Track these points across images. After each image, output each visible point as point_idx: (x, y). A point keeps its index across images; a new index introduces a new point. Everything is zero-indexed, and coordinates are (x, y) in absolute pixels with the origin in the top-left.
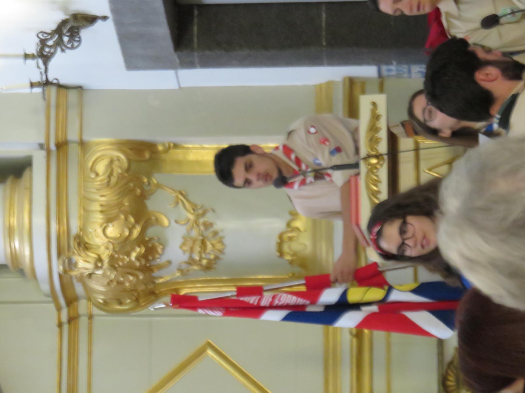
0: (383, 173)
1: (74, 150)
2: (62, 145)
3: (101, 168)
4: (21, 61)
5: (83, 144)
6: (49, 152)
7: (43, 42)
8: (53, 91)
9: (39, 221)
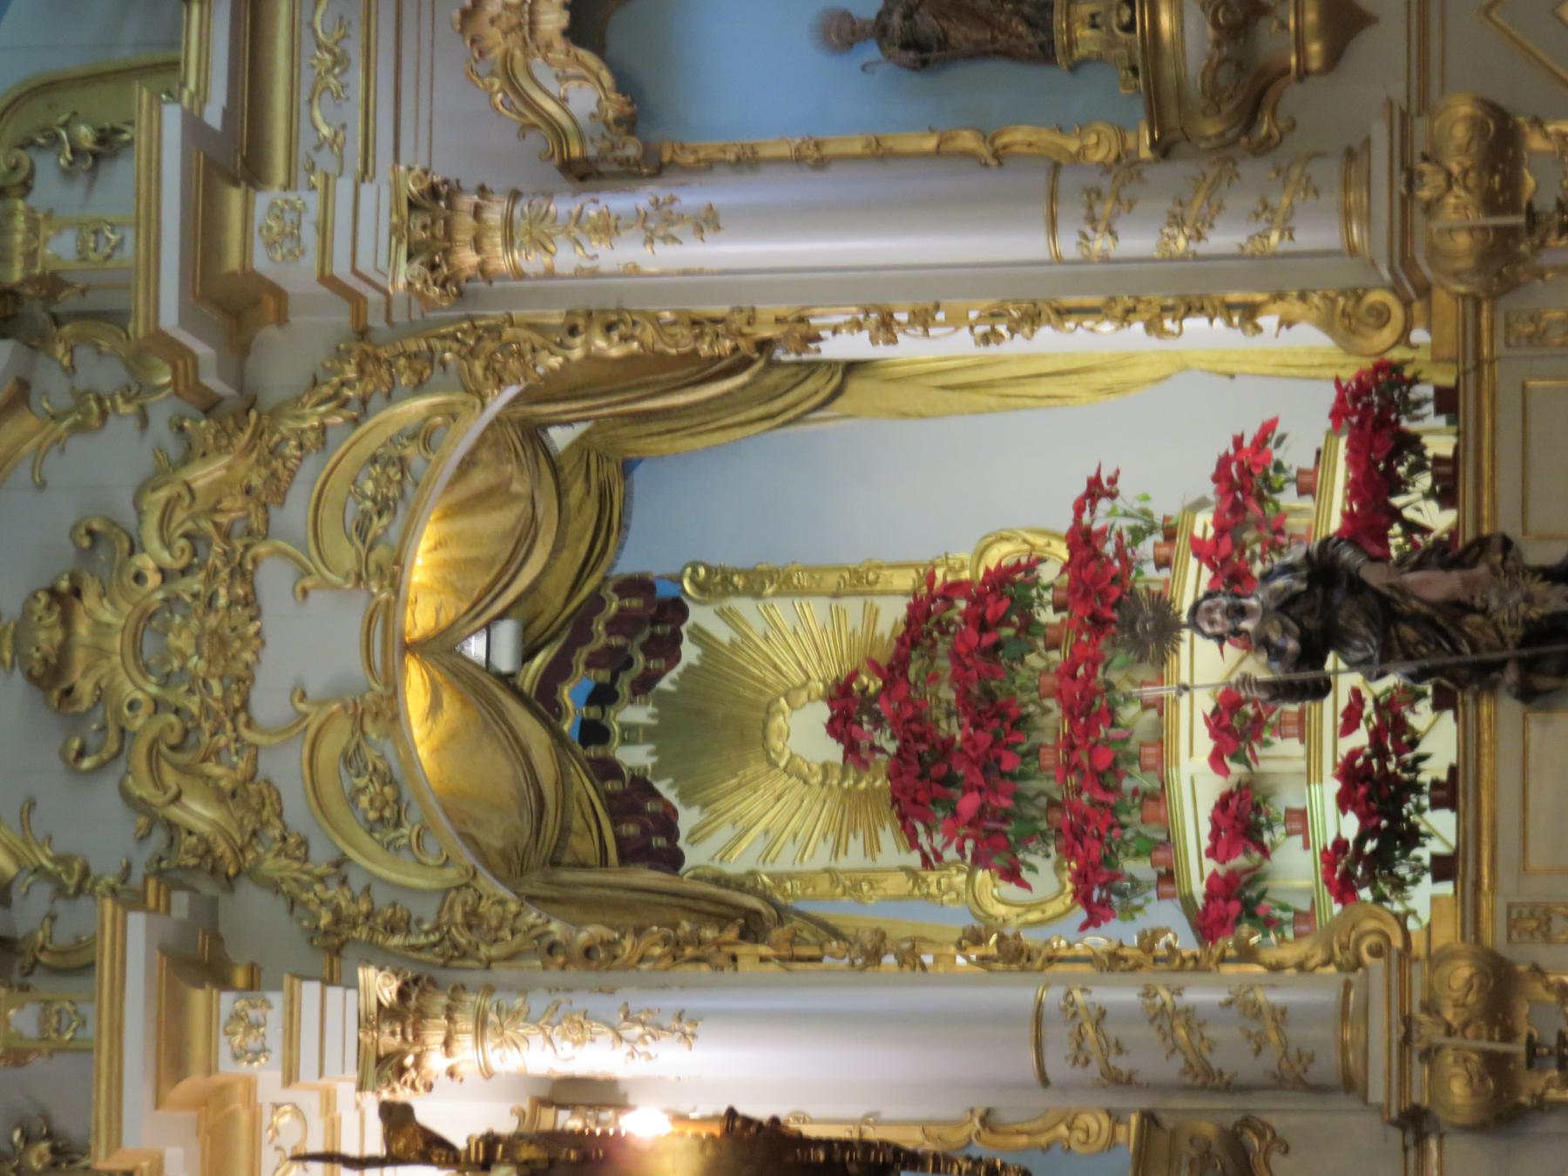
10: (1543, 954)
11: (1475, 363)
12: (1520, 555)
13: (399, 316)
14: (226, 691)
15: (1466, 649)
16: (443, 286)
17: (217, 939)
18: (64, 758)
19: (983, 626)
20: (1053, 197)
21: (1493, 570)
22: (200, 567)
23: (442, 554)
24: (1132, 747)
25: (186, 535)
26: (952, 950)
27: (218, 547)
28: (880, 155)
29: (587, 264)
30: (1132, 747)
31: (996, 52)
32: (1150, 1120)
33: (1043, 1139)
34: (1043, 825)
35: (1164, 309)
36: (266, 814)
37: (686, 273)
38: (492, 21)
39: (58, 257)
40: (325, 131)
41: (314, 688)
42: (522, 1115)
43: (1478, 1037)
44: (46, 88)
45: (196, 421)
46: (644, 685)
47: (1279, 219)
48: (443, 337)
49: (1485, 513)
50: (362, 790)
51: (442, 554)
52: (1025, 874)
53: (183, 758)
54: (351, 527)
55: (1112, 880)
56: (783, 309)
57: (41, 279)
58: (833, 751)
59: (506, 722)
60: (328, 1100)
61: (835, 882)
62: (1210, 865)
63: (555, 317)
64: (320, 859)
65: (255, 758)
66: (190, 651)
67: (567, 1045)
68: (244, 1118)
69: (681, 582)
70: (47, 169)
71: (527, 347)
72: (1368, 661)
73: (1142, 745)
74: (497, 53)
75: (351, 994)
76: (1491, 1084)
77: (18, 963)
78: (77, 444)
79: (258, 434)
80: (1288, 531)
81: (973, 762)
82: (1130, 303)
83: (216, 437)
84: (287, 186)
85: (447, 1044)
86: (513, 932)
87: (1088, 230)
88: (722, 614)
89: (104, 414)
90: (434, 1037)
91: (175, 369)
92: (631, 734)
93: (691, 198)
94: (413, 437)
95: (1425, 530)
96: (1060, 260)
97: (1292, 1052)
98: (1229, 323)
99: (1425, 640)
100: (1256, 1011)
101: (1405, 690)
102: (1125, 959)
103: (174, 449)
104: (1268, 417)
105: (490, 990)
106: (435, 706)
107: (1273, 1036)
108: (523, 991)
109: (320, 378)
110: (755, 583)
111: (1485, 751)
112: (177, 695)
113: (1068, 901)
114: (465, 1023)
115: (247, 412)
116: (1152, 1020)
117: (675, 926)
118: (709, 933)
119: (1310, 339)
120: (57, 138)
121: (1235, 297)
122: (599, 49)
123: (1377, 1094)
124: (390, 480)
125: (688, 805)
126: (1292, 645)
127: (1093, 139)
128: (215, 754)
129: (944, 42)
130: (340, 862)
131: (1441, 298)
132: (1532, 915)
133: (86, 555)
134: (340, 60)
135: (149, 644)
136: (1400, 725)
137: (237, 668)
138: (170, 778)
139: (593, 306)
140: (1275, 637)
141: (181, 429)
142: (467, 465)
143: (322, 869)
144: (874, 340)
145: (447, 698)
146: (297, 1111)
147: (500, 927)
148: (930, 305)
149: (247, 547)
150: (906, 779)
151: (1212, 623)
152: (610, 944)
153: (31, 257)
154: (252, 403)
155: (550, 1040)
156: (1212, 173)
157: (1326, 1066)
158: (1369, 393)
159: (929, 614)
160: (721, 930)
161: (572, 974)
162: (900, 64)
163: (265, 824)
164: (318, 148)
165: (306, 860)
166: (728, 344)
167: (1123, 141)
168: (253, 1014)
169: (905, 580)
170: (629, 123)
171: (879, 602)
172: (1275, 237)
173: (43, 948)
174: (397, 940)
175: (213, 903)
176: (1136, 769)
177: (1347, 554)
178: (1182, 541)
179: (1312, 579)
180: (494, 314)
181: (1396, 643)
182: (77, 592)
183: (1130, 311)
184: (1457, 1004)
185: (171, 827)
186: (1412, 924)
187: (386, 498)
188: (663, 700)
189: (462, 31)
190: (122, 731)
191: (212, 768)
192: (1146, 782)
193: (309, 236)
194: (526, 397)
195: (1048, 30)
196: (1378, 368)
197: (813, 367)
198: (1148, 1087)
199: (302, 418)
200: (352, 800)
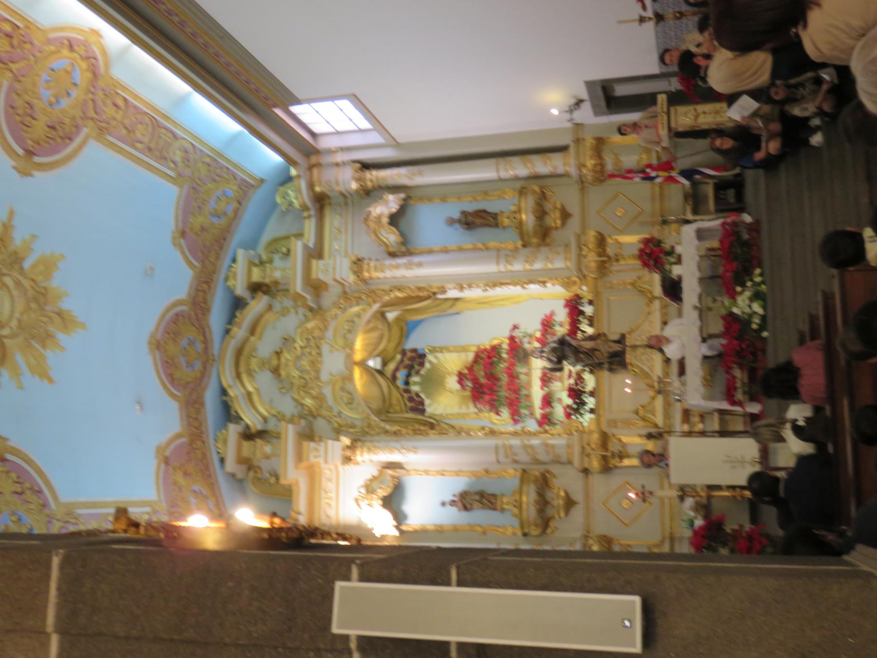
0: (665, 118)
5: (584, 139)
10: (615, 431)
11: (597, 293)
17: (312, 430)
28: (461, 249)
32: (524, 471)
44: (276, 240)
46: (417, 373)
52: (500, 413)
53: (305, 389)
55: (519, 414)
56: (438, 284)
58: (457, 386)
62: (542, 412)
64: (335, 411)
70: (276, 257)
90: (358, 453)
92: (415, 383)
93: (416, 259)
94: (355, 315)
96: (501, 272)
100: (546, 445)
105: (371, 441)
106: (361, 377)
108: (379, 441)
110: (442, 349)
118: (422, 428)
120: (277, 251)
121: (541, 279)
126: (555, 359)
128: (312, 388)
130: (340, 413)
131: (589, 279)
133: (284, 344)
134: (340, 231)
142: (369, 322)
146: (330, 470)
152: (399, 431)
154: (320, 308)
157: (564, 458)
169: (474, 349)
174: (352, 430)
180: (373, 287)
182: (281, 352)
184: (595, 443)
185: (302, 405)
188: (422, 376)
193: (331, 270)
194: (383, 306)
197: (447, 300)
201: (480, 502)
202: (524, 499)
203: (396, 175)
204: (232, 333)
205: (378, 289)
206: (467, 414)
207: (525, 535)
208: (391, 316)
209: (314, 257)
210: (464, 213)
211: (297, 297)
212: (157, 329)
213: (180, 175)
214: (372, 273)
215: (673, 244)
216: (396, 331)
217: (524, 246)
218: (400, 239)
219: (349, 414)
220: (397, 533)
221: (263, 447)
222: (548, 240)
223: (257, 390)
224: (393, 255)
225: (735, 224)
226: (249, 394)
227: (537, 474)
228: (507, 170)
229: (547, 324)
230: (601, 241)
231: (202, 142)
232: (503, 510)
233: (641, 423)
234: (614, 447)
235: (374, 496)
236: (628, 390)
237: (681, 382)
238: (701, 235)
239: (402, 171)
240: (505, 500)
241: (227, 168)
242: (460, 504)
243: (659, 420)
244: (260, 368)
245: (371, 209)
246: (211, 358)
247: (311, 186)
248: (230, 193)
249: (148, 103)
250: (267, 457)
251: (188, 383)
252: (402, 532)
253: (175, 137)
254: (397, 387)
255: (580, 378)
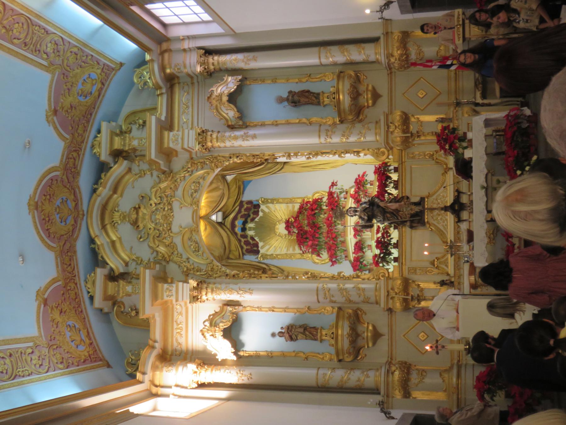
0: (461, 29)
1: (390, 34)
2: (387, 33)
3: (396, 38)
4: (376, 13)
5: (392, 33)
6: (384, 35)
7: (381, 8)
8: (385, 20)
9: (382, 51)
10: (414, 277)
11: (402, 163)
12: (410, 200)
13: (198, 155)
14: (167, 226)
15: (400, 218)
16: (206, 149)
17: (165, 272)
18: (137, 238)
19: (312, 210)
20: (320, 131)
21: (405, 204)
22: (162, 203)
23: (207, 200)
24: (339, 233)
25: (159, 197)
26: (302, 275)
27: (165, 199)
28: (288, 123)
29: (232, 145)
30: (339, 233)
31: (309, 103)
32: (340, 309)
33: (319, 312)
34: (324, 247)
35: (342, 152)
36: (174, 249)
37: (251, 146)
38: (214, 99)
39: (134, 145)
40: (185, 120)
41: (183, 226)
42: (220, 307)
43: (402, 295)
44: (134, 113)
45: (161, 175)
46: (253, 220)
47: (363, 135)
48: (207, 159)
49: (404, 191)
50: (191, 245)
51: (207, 200)
52: (321, 255)
53: (158, 239)
54: (190, 195)
56: (270, 153)
57: (131, 149)
58: (286, 232)
59: (219, 232)
60: (186, 303)
61: (287, 256)
62: (354, 255)
63: (227, 155)
64: (184, 257)
65: (172, 239)
66: (160, 218)
67: (229, 295)
68: (171, 306)
69: (259, 202)
70: (135, 127)
71: (222, 161)
72: (380, 221)
73: (341, 232)
74: (214, 105)
75: (188, 284)
76: (404, 304)
77: (130, 277)
78: (140, 179)
79: (173, 178)
80: (368, 192)
81: (311, 235)
82: (335, 151)
83: (165, 178)
84: (178, 131)
85: (206, 294)
86: (220, 272)
87: (326, 137)
88: (267, 207)
89: (145, 174)
90: (204, 293)
91: (156, 166)
92: (250, 229)
93: (251, 132)
94: (201, 178)
95: (392, 194)
96: (321, 143)
97: (366, 297)
98: (354, 155)
99: (392, 217)
100: (359, 289)
101: (388, 226)
102: (335, 277)
103: (157, 180)
104: (364, 171)
105: (215, 283)
106: (206, 229)
107: (362, 294)
108: (220, 284)
109: (184, 166)
110: (273, 201)
111: (404, 237)
112: (158, 227)
113: (327, 260)
114: (209, 290)
115: (170, 173)
116: (339, 291)
117: (250, 271)
118: (256, 272)
119: (370, 158)
120: (136, 123)
122: (235, 105)
123: (382, 305)
124: (197, 186)
125: (261, 242)
126: (366, 218)
127: (328, 120)
128: (165, 238)
129: (299, 102)
130: (188, 259)
131: (395, 150)
132: (413, 270)
133: (142, 201)
134: (188, 107)
135: (153, 217)
136: (387, 232)
137: (169, 222)
138: (157, 242)
139: (234, 153)
140: (363, 216)
141: (158, 177)
142: (211, 183)
143: (185, 260)
144: (287, 159)
145: (208, 227)
146: (180, 305)
147: (217, 271)
148: (297, 151)
149: (171, 199)
150: (299, 238)
151: (351, 213)
152: (238, 274)
153: (129, 145)
154: (171, 172)
155: (225, 293)
156: (350, 126)
157: (373, 299)
158: (381, 168)
159: (303, 207)
160: (259, 272)
161: (231, 280)
162: (291, 106)
163: (174, 251)
164: (183, 124)
165: (182, 258)
166: (259, 160)
167: (334, 121)
168: (170, 288)
169: (300, 201)
170: (240, 118)
171: (295, 204)
172: (362, 138)
173: (134, 274)
174: (198, 273)
175: (165, 266)
176: (340, 237)
177: (376, 200)
178: (349, 194)
179: (370, 205)
180: (216, 154)
181: (386, 218)
182: (139, 208)
183: (336, 153)
184: (398, 288)
185: (157, 252)
186: (390, 271)
187: (196, 190)
188: (256, 222)
189: (208, 101)
190: (148, 234)
191: (164, 241)
192: (342, 239)
193: (180, 140)
195: (319, 99)
196: (383, 163)
197: (278, 163)
198: (339, 303)
199: (180, 174)
200: (190, 247)
201: (304, 333)
202: (340, 332)
203: (234, 60)
204: (98, 192)
205: (219, 156)
206: (294, 255)
207: (340, 361)
208: (229, 178)
209: (166, 129)
210: (290, 92)
211: (152, 163)
212: (35, 193)
213: (52, 64)
214: (214, 143)
215: (466, 131)
216: (234, 188)
217: (342, 122)
218: (237, 115)
219: (196, 260)
220: (235, 358)
221: (125, 288)
222: (361, 118)
223: (120, 239)
224: (232, 127)
225: (516, 117)
226: (113, 243)
227: (350, 311)
228: (327, 57)
229: (360, 183)
230: (406, 119)
231: (70, 36)
232: (322, 341)
233: (436, 271)
234: (414, 291)
235: (217, 329)
236: (426, 253)
237: (470, 246)
238: (487, 123)
239: (240, 56)
240: (324, 333)
241: (92, 56)
242: (287, 335)
243: (451, 271)
244: (122, 221)
245: (214, 89)
246: (81, 213)
247: (163, 68)
248: (94, 76)
249: (22, 6)
250: (129, 295)
251: (63, 235)
252: (239, 357)
253: (47, 32)
254: (236, 234)
255: (386, 233)
